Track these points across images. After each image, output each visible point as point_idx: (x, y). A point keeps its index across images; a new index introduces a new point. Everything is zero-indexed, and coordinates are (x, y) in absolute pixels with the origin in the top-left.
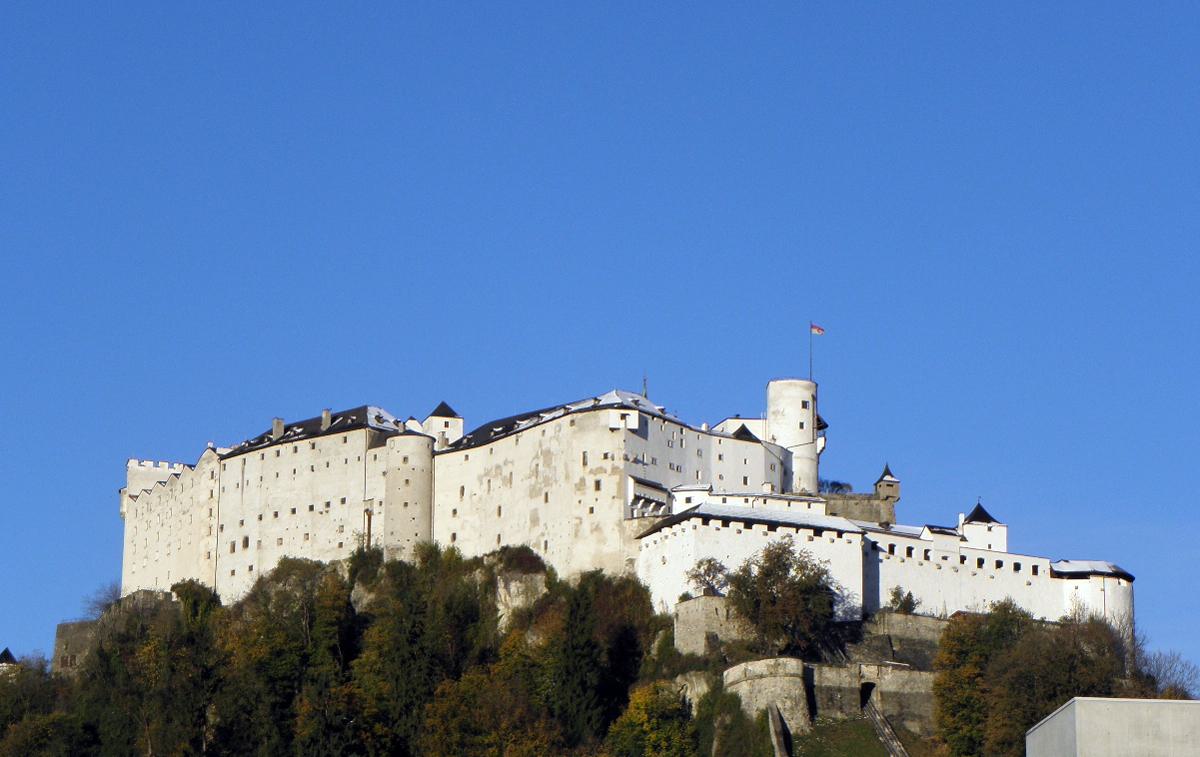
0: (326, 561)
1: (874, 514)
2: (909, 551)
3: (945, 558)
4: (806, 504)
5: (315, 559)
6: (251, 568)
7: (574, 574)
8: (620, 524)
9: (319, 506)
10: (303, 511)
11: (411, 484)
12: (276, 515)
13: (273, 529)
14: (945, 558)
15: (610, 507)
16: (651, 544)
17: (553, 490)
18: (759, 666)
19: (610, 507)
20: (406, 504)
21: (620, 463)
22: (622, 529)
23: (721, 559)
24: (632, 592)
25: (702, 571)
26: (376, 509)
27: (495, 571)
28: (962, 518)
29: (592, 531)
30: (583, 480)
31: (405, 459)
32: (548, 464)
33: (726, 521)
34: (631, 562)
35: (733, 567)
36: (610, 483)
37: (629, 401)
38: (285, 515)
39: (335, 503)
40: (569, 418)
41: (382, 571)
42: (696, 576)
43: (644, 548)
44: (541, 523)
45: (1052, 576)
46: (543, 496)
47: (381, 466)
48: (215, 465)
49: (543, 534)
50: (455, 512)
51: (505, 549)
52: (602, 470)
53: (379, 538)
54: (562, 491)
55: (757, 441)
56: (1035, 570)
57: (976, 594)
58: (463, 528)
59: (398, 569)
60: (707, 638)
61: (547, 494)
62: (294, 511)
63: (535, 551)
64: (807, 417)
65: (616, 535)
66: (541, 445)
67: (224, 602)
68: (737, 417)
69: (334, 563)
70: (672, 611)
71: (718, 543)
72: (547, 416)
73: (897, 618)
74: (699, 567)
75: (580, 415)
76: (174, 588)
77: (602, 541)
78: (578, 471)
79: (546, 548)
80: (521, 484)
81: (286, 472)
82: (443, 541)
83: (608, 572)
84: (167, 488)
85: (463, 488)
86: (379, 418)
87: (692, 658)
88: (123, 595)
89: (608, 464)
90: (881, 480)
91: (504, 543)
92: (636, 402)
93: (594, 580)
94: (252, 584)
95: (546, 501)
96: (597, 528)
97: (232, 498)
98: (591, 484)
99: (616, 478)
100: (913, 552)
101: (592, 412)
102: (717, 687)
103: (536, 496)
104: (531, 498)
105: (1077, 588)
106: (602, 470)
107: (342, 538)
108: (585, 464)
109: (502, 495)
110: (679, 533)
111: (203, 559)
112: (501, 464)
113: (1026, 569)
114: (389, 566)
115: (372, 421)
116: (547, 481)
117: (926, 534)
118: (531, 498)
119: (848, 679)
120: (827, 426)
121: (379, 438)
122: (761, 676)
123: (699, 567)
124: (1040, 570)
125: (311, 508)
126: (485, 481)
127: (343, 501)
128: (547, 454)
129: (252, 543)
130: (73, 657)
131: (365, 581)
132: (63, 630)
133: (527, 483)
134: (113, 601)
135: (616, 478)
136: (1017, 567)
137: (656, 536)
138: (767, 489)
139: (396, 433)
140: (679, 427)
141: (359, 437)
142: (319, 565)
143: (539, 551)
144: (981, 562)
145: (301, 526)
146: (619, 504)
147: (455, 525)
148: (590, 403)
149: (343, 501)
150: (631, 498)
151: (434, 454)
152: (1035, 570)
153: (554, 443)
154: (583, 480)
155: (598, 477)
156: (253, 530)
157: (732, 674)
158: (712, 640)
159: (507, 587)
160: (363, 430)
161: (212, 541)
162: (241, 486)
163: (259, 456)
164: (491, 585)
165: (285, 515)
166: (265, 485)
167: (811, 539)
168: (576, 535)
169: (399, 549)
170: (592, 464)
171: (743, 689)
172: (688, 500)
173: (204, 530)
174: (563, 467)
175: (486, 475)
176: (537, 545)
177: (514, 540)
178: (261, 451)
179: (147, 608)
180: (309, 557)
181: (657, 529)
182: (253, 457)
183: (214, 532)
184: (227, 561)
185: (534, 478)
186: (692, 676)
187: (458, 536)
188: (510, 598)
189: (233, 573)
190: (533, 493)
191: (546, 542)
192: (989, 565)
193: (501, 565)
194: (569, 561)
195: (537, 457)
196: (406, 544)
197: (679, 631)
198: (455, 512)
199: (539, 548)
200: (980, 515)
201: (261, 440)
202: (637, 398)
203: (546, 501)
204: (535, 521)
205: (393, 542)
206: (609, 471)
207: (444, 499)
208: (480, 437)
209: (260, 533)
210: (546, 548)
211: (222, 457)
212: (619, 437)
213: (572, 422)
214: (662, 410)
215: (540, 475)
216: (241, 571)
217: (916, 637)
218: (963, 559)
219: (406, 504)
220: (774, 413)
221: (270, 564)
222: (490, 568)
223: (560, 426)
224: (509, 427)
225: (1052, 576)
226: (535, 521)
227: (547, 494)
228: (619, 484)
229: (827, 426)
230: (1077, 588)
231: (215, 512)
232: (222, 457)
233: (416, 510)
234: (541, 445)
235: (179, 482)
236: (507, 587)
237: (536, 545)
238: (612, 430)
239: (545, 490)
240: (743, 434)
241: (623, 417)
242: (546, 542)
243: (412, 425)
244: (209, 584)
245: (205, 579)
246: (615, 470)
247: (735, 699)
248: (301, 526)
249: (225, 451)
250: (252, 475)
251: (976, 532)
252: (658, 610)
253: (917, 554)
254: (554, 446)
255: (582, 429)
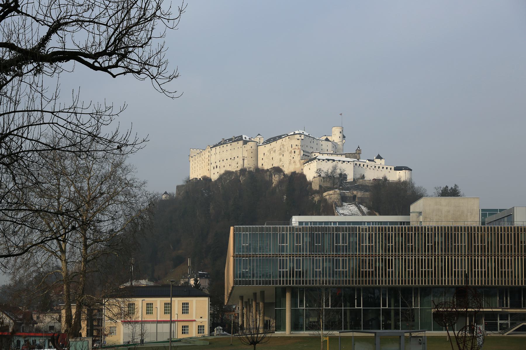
0: (234, 171)
1: (355, 158)
2: (364, 165)
3: (371, 167)
4: (341, 156)
5: (232, 170)
6: (218, 172)
7: (289, 173)
8: (299, 161)
9: (233, 158)
10: (229, 159)
11: (253, 153)
12: (223, 160)
13: (223, 164)
14: (371, 167)
15: (298, 157)
16: (307, 165)
17: (285, 154)
18: (331, 192)
19: (298, 157)
20: (252, 157)
21: (300, 147)
22: (300, 162)
23: (322, 169)
24: (303, 176)
25: (318, 171)
26: (245, 159)
27: (272, 172)
28: (375, 157)
29: (293, 163)
30: (291, 151)
31: (251, 147)
32: (283, 147)
33: (323, 160)
34: (302, 169)
35: (325, 170)
36: (297, 152)
37: (301, 133)
38: (225, 160)
39: (236, 157)
40: (288, 137)
41: (246, 173)
42: (316, 172)
43: (305, 166)
44: (282, 161)
45: (394, 170)
46: (282, 155)
47: (246, 149)
48: (209, 149)
49: (282, 164)
50: (262, 159)
51: (274, 167)
52: (295, 149)
53: (246, 166)
54: (287, 154)
55: (330, 141)
56: (391, 169)
57: (378, 175)
58: (264, 162)
59: (250, 172)
60: (319, 186)
61: (283, 154)
62: (227, 159)
63: (281, 167)
64: (341, 135)
65: (299, 163)
66: (282, 143)
67: (213, 180)
68: (325, 136)
69: (236, 171)
70: (311, 180)
71: (321, 164)
72: (283, 136)
73: (361, 180)
74: (317, 170)
75: (291, 136)
76: (201, 177)
77: (295, 165)
78: (290, 149)
79: (283, 167)
80: (277, 152)
81: (225, 151)
82: (260, 166)
83: (297, 172)
84: (199, 155)
85: (264, 153)
86: (245, 138)
87: (316, 190)
88: (190, 179)
89: (297, 147)
90: (357, 149)
91: (273, 166)
92: (303, 133)
93: (294, 173)
94: (218, 176)
95: (283, 156)
96: (294, 162)
97: (213, 157)
98: (293, 152)
99: (299, 150)
100: (365, 165)
101: (293, 135)
102: (322, 196)
103: (281, 155)
104: (280, 155)
105: (400, 173)
106: (295, 149)
107: (238, 165)
108: (292, 147)
109: (273, 155)
110: (313, 162)
111: (208, 172)
112: (273, 148)
113: (389, 169)
114: (248, 171)
115: (244, 139)
116: (283, 152)
117: (368, 162)
118: (280, 155)
119: (350, 194)
120: (345, 137)
121: (245, 142)
122: (331, 194)
123: (317, 170)
124: (392, 169)
125: (231, 159)
126: (269, 151)
127: (238, 157)
128: (283, 145)
129: (218, 167)
130: (180, 193)
131: (243, 175)
132: (178, 187)
133: (279, 152)
134: (189, 181)
135: (299, 150)
136: (387, 168)
137: (308, 163)
138: (332, 152)
139: (249, 141)
140: (313, 138)
141: (241, 143)
142: (233, 172)
143: (282, 168)
144: (379, 167)
145: (229, 163)
146: (299, 156)
147: (262, 162)
148: (293, 133)
149: (238, 157)
150: (302, 155)
151: (258, 146)
152: (391, 169)
153: (285, 142)
154: (291, 151)
155: (295, 150)
156: (218, 164)
157: (325, 194)
158: (320, 186)
159: (274, 176)
160: (242, 141)
161: (209, 166)
162: (215, 154)
163: (219, 147)
164: (271, 176)
165: (225, 160)
166: (220, 153)
167: (342, 163)
168: (290, 164)
169: (251, 168)
170: (293, 147)
171: (327, 197)
172: (315, 155)
173: (208, 164)
174: (287, 148)
175: (269, 150)
176: (281, 166)
177: (276, 165)
178: (220, 146)
179: (197, 181)
180: (231, 170)
181: (308, 162)
182: (218, 148)
183: (210, 165)
184: (213, 171)
185: (280, 151)
186: (316, 195)
187: (263, 164)
188: (276, 179)
189: (214, 174)
190: (280, 154)
191: (283, 165)
192: (381, 168)
193: (273, 171)
194: (288, 169)
195: (281, 146)
196: (252, 167)
197: (313, 185)
198: (262, 159)
199: (282, 167)
200: (379, 157)
201: (219, 143)
202: (303, 131)
203: (283, 156)
204: (281, 161)
205: (249, 166)
206: (297, 149)
207: (260, 156)
208: (269, 141)
209: (220, 165)
210: (283, 167)
211: (211, 148)
212: (300, 141)
213: (289, 138)
214: (309, 134)
215: (282, 150)
216: (216, 173)
217: (365, 185)
218: (375, 167)
219: (252, 157)
220: (334, 134)
221: (222, 172)
222: (271, 171)
223: (286, 138)
224: (275, 139)
225: (394, 170)
226: (281, 161)
227: (283, 154)
228: (299, 152)
229: (345, 137)
230: (400, 173)
231: (210, 160)
232: (211, 148)
233: (254, 159)
234: (282, 143)
235: (202, 153)
236: (274, 176)
237: (281, 166)
238: (298, 139)
239: (283, 153)
240: (327, 140)
241: (300, 136)
242: (283, 165)
243: (252, 139)
244: (209, 176)
245: (208, 176)
246: (298, 148)
247: (326, 200)
248: (229, 163)
249: (212, 146)
250: (218, 151)
251: (378, 161)
252: (308, 180)
253: (365, 166)
254: (285, 143)
255: (291, 139)
